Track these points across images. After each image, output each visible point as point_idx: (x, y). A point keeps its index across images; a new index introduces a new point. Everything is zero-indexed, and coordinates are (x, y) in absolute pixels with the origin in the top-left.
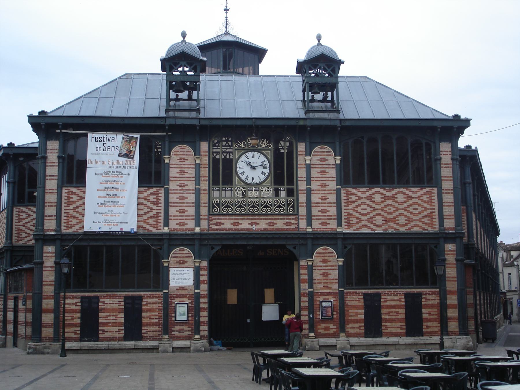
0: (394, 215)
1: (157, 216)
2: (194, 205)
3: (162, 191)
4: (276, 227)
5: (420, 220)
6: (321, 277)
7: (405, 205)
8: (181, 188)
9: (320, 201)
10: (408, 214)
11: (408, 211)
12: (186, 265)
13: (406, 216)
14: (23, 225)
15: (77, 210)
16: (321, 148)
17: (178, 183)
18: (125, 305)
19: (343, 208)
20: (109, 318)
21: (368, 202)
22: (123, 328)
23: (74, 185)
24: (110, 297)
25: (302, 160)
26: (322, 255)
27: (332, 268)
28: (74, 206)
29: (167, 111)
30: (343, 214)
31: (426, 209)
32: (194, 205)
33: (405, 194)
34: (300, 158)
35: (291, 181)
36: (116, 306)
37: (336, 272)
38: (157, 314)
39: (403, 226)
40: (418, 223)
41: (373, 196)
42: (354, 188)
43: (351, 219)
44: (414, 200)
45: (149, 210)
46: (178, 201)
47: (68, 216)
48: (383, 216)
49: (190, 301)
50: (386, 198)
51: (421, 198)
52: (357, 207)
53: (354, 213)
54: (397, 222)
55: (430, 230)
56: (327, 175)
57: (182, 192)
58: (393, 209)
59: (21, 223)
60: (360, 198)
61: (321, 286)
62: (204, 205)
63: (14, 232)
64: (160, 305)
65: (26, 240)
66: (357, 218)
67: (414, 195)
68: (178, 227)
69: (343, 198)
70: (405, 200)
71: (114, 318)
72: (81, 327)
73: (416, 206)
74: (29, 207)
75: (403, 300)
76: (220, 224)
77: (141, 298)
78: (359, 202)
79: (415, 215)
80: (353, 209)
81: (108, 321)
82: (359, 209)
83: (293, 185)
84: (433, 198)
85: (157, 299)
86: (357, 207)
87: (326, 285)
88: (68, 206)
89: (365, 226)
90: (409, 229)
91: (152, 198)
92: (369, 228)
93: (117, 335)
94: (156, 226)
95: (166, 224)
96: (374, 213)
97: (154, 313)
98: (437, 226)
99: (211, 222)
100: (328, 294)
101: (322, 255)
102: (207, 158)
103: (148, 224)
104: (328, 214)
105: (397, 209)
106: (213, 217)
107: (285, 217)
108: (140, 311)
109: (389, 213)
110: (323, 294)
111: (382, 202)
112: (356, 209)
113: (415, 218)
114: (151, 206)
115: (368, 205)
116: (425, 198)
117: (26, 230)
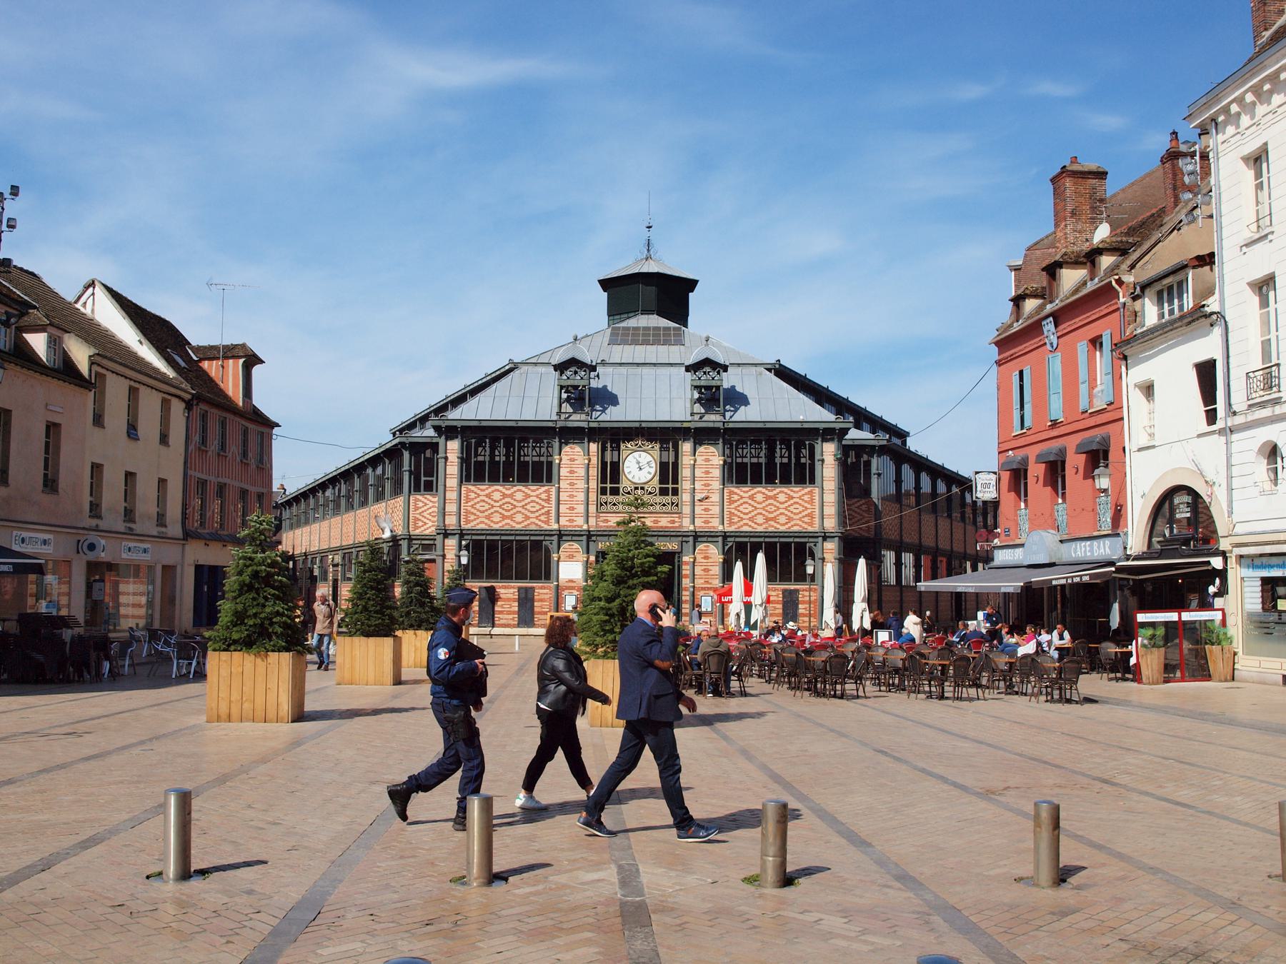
0: (775, 514)
1: (548, 513)
3: (553, 490)
4: (660, 524)
5: (800, 519)
6: (702, 573)
7: (786, 505)
10: (789, 514)
11: (789, 511)
12: (575, 559)
13: (786, 515)
14: (420, 514)
16: (705, 448)
17: (568, 482)
21: (750, 501)
24: (505, 587)
25: (686, 460)
28: (472, 503)
29: (559, 413)
30: (725, 513)
31: (806, 508)
33: (786, 494)
35: (675, 481)
36: (511, 596)
39: (784, 525)
40: (798, 522)
42: (737, 487)
44: (795, 500)
46: (568, 499)
47: (467, 512)
48: (764, 515)
50: (768, 498)
52: (739, 506)
53: (736, 512)
55: (810, 529)
56: (711, 475)
58: (774, 508)
59: (418, 512)
61: (702, 581)
63: (411, 521)
65: (422, 529)
66: (739, 517)
67: (795, 495)
68: (568, 523)
69: (725, 497)
73: (797, 506)
76: (607, 521)
77: (533, 589)
78: (741, 501)
79: (795, 514)
80: (735, 508)
82: (741, 508)
83: (677, 484)
86: (739, 506)
89: (746, 524)
90: (789, 528)
91: (543, 496)
92: (750, 526)
93: (512, 623)
94: (547, 522)
96: (756, 512)
98: (817, 526)
100: (709, 589)
102: (596, 459)
103: (540, 520)
105: (778, 508)
107: (669, 515)
108: (533, 600)
109: (770, 512)
110: (703, 589)
111: (764, 501)
113: (795, 517)
114: (543, 503)
115: (750, 504)
116: (806, 498)
117: (423, 519)
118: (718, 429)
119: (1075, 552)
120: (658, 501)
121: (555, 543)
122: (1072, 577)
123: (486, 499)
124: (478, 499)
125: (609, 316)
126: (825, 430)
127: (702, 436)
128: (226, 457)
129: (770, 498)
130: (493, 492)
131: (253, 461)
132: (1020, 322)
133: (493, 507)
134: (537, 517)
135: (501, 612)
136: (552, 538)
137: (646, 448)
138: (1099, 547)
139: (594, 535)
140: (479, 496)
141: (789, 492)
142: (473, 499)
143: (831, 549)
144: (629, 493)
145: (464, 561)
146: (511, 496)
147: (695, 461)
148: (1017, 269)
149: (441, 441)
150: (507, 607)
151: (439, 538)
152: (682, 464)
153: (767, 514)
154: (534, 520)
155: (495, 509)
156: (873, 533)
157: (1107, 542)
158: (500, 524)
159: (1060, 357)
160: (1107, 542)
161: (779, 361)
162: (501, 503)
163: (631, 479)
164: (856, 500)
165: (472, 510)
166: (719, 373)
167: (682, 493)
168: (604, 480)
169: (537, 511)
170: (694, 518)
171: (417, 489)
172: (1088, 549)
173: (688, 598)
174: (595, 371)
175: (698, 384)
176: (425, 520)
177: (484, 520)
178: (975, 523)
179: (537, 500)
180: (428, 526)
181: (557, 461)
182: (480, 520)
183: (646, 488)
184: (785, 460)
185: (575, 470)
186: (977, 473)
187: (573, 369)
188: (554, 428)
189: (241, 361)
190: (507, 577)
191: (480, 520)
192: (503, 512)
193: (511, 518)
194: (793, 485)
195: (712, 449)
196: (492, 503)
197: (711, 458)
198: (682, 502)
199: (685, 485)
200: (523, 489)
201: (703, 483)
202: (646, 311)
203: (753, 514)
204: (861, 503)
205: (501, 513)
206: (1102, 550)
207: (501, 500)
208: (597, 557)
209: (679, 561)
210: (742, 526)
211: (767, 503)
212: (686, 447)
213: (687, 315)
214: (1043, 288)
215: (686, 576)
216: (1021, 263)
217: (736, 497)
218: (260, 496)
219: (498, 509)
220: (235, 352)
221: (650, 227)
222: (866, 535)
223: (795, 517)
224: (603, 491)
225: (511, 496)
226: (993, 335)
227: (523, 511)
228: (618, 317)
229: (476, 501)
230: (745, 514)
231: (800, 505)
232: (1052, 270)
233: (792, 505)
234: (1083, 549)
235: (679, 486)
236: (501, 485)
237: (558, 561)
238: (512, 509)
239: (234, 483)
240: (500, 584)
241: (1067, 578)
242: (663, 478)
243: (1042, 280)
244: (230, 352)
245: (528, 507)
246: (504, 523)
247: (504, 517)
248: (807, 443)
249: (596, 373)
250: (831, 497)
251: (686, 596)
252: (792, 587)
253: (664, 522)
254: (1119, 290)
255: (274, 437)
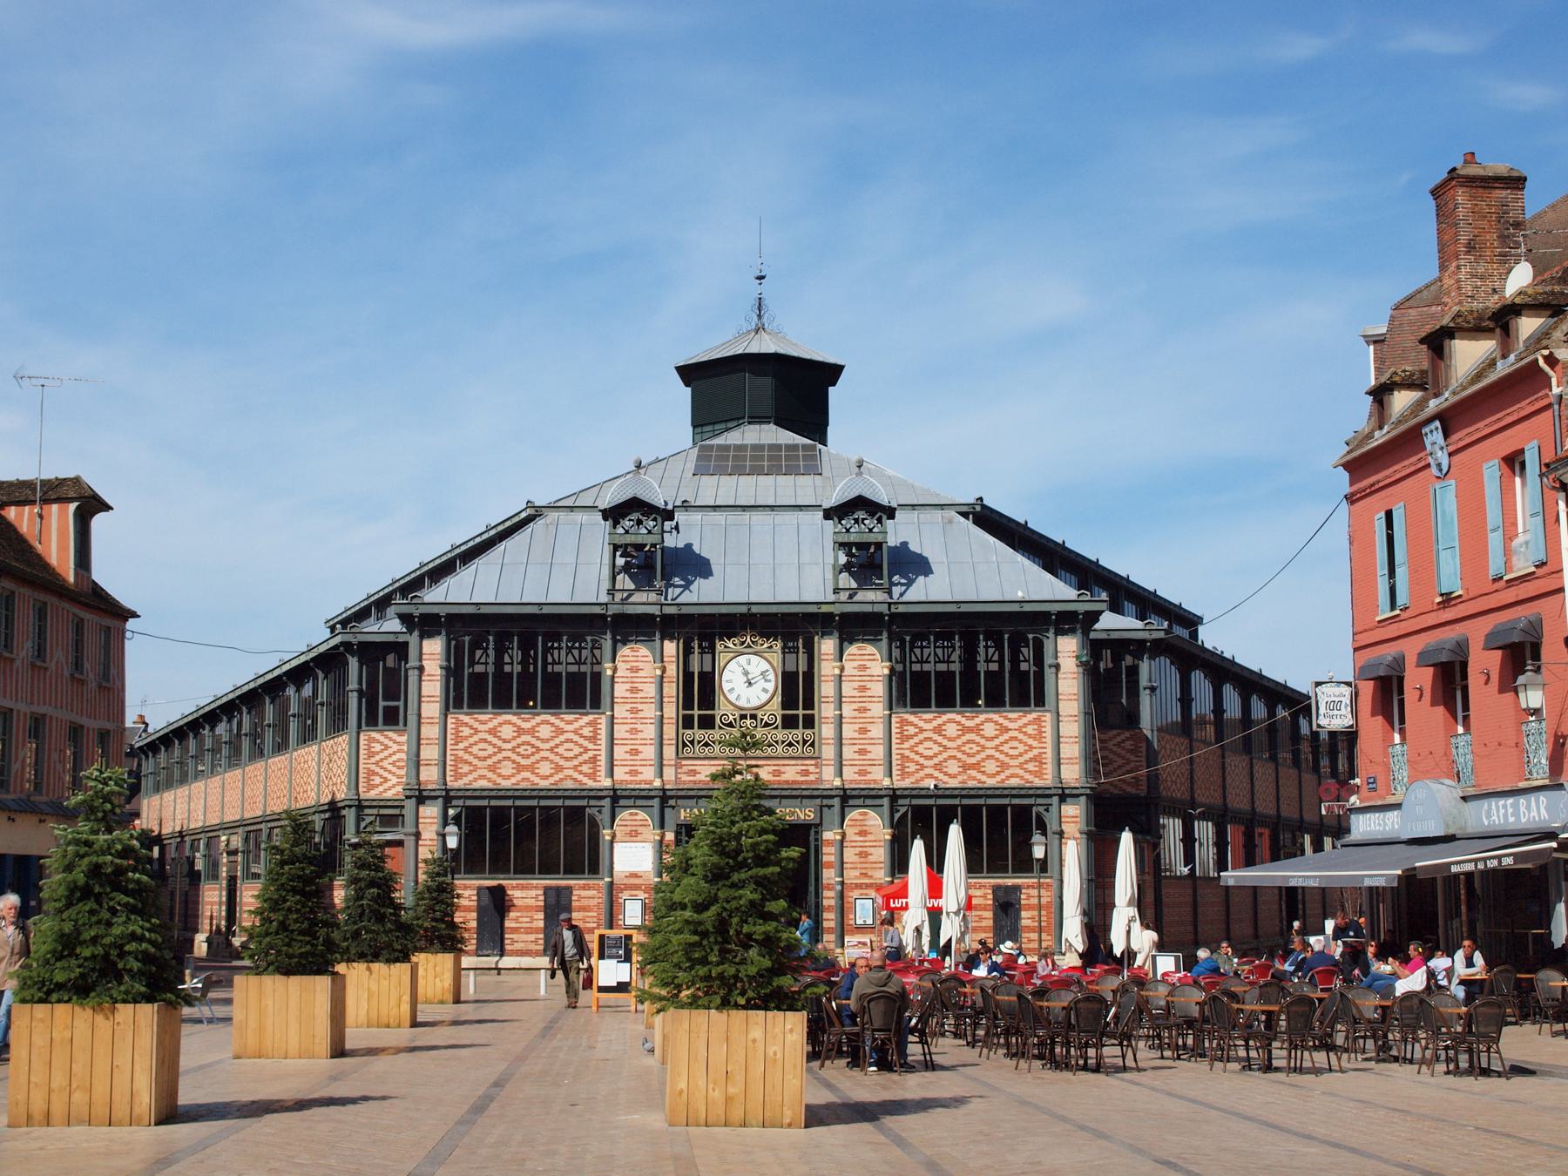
0: (978, 757)
1: (594, 760)
2: (652, 742)
3: (603, 722)
4: (784, 777)
5: (1020, 766)
6: (856, 859)
7: (997, 741)
8: (632, 716)
9: (856, 735)
10: (1002, 757)
11: (1002, 752)
13: (997, 760)
14: (377, 763)
15: (470, 750)
16: (859, 648)
17: (628, 707)
18: (545, 901)
19: (894, 746)
20: (521, 920)
21: (935, 737)
22: (542, 936)
23: (465, 710)
24: (523, 888)
25: (827, 668)
26: (858, 823)
27: (874, 844)
28: (466, 744)
29: (612, 591)
30: (894, 757)
31: (1031, 748)
32: (652, 742)
33: (996, 723)
34: (824, 664)
35: (809, 704)
36: (532, 902)
37: (882, 851)
38: (595, 914)
39: (993, 775)
41: (944, 727)
42: (912, 713)
43: (907, 765)
45: (582, 750)
46: (627, 735)
47: (457, 760)
48: (959, 760)
49: (646, 895)
50: (966, 730)
51: (1024, 730)
52: (917, 745)
53: (912, 755)
54: (983, 769)
55: (1038, 782)
57: (634, 721)
59: (373, 760)
60: (922, 730)
61: (857, 873)
62: (669, 742)
63: (361, 775)
64: (600, 901)
65: (381, 789)
66: (917, 763)
67: (1011, 726)
68: (627, 777)
69: (894, 730)
70: (997, 732)
71: (528, 920)
72: (478, 934)
73: (1015, 744)
74: (386, 733)
75: (991, 897)
76: (695, 773)
77: (569, 889)
78: (921, 737)
79: (1012, 757)
80: (911, 749)
81: (518, 925)
82: (920, 749)
83: (813, 709)
84: (1043, 729)
85: (595, 892)
86: (917, 745)
87: (864, 871)
88: (456, 744)
90: (1003, 781)
91: (586, 732)
93: (533, 947)
94: (592, 776)
95: (611, 774)
96: (945, 755)
97: (590, 914)
98: (1049, 777)
99: (679, 771)
100: (868, 886)
101: (858, 823)
102: (674, 667)
104: (869, 756)
105: (984, 748)
106: (684, 762)
107: (800, 762)
109: (969, 755)
110: (859, 886)
111: (959, 737)
112: (916, 749)
113: (1012, 762)
114: (585, 743)
115: (935, 742)
116: (1030, 730)
117: (381, 772)
118: (880, 615)
119: (1489, 816)
120: (780, 737)
121: (607, 811)
122: (1484, 860)
123: (490, 738)
124: (476, 738)
125: (695, 426)
126: (1060, 614)
127: (852, 627)
128: (46, 669)
129: (970, 730)
130: (500, 725)
131: (91, 675)
132: (1386, 428)
133: (500, 750)
134: (575, 768)
135: (515, 930)
136: (602, 803)
137: (758, 648)
138: (1528, 808)
139: (672, 797)
140: (476, 731)
141: (1001, 720)
142: (466, 738)
143: (1073, 816)
144: (730, 725)
145: (452, 843)
146: (532, 732)
147: (842, 669)
148: (1378, 341)
149: (413, 639)
150: (524, 922)
151: (410, 805)
152: (820, 676)
153: (964, 757)
154: (571, 772)
155: (504, 754)
156: (1145, 788)
157: (1541, 798)
158: (513, 780)
159: (1454, 486)
160: (1541, 798)
161: (981, 499)
162: (514, 743)
163: (733, 700)
164: (1115, 732)
165: (466, 757)
166: (880, 521)
167: (820, 723)
168: (688, 704)
169: (576, 757)
170: (841, 765)
171: (372, 721)
172: (1510, 810)
173: (832, 902)
174: (672, 519)
175: (846, 540)
176: (386, 774)
177: (485, 772)
178: (1316, 768)
179: (576, 738)
180: (389, 784)
181: (609, 672)
182: (480, 772)
183: (760, 716)
184: (994, 667)
185: (640, 686)
186: (1318, 684)
187: (635, 516)
188: (603, 617)
189: (73, 506)
190: (524, 869)
191: (480, 772)
192: (519, 759)
193: (531, 768)
194: (1008, 708)
195: (870, 649)
196: (500, 743)
197: (868, 664)
198: (820, 738)
199: (826, 711)
200: (552, 719)
201: (855, 706)
202: (757, 419)
203: (941, 758)
204: (1123, 737)
205: (514, 762)
206: (1534, 813)
207: (514, 738)
208: (678, 834)
209: (816, 840)
210: (922, 779)
211: (964, 739)
212: (827, 646)
213: (826, 424)
214: (1423, 372)
215: (830, 865)
216: (1384, 330)
217: (912, 730)
218: (104, 736)
219: (509, 754)
220: (63, 492)
221: (762, 278)
222: (1133, 791)
223: (1012, 762)
224: (688, 723)
225: (532, 732)
226: (1340, 451)
227: (552, 756)
228: (709, 428)
229: (472, 740)
230: (927, 758)
231: (1021, 741)
232: (1437, 342)
233: (1006, 742)
234: (1502, 811)
235: (816, 712)
236: (514, 714)
237: (612, 842)
238: (533, 754)
239: (60, 714)
240: (514, 882)
241: (1476, 861)
242: (789, 700)
243: (1421, 359)
244: (53, 491)
245: (560, 750)
246: (519, 777)
247: (520, 768)
248: (1030, 636)
249: (674, 523)
250: (1072, 729)
251: (829, 898)
252: (1010, 882)
253: (791, 773)
254: (1551, 373)
255: (128, 635)
